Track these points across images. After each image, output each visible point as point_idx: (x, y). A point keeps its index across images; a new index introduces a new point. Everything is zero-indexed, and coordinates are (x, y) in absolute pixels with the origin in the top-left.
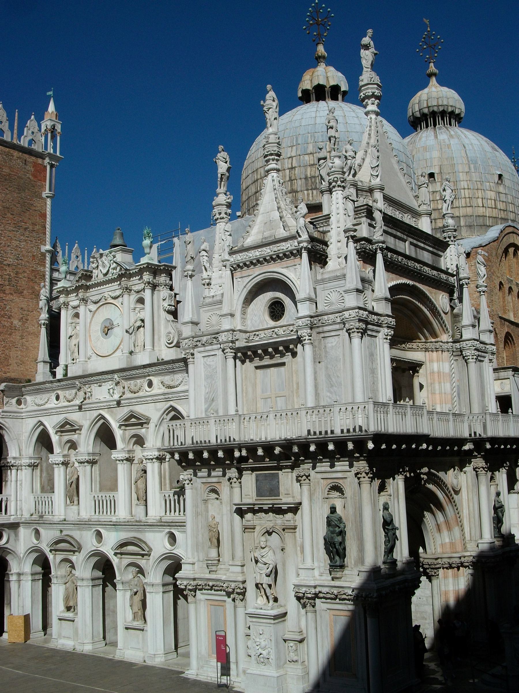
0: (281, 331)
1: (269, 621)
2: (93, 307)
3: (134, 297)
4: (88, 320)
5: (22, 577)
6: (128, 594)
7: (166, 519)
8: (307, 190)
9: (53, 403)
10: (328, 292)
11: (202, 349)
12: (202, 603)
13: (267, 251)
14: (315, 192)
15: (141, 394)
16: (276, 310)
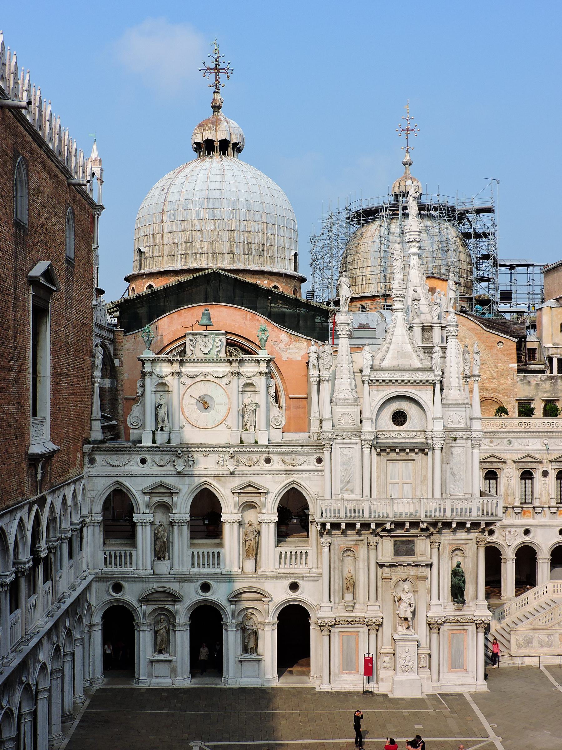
0: (405, 436)
1: (413, 643)
2: (189, 382)
3: (243, 381)
4: (182, 393)
5: (95, 629)
6: (239, 633)
7: (281, 571)
8: (244, 254)
9: (134, 465)
10: (451, 413)
11: (340, 442)
12: (336, 635)
13: (406, 376)
14: (250, 257)
15: (256, 468)
16: (399, 418)
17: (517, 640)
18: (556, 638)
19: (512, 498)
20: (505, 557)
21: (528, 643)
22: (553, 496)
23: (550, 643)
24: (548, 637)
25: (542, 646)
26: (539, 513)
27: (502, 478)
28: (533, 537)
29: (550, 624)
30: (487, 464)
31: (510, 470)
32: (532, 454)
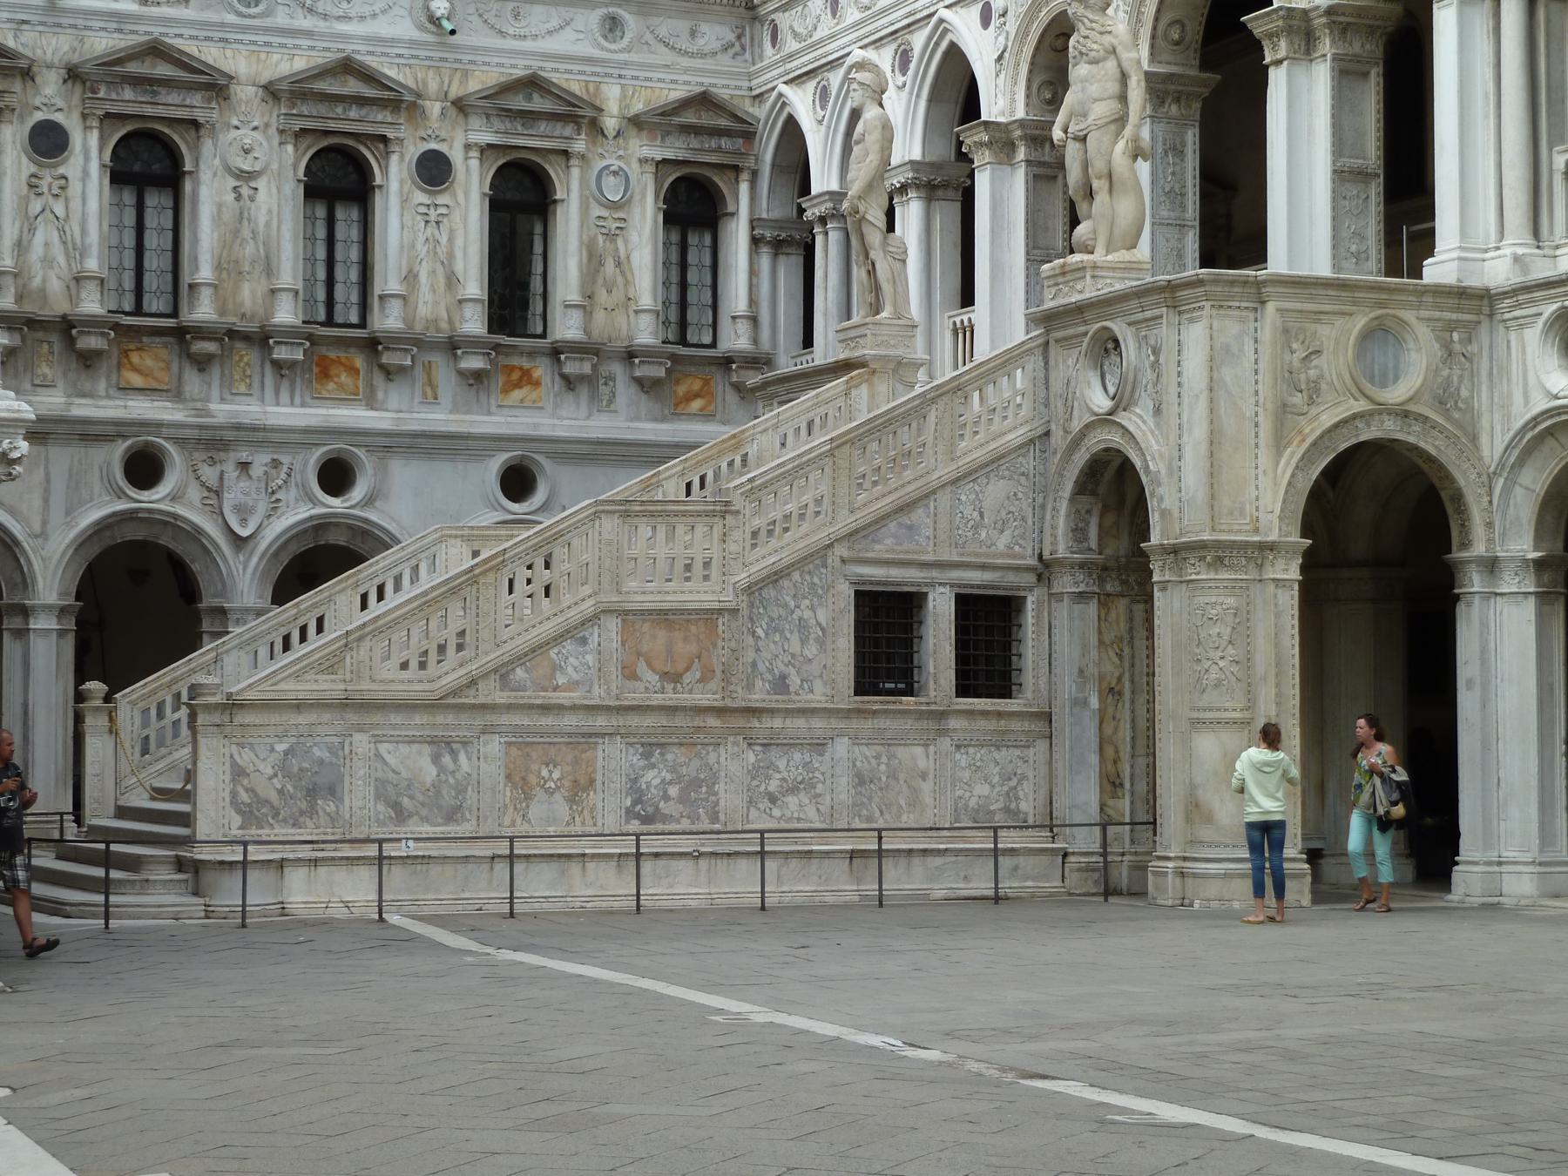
17: (238, 773)
18: (487, 760)
19: (262, 287)
20: (216, 602)
21: (312, 793)
22: (475, 285)
23: (448, 799)
24: (436, 759)
25: (401, 815)
26: (402, 370)
27: (205, 175)
28: (369, 501)
29: (449, 674)
30: (128, 94)
31: (247, 137)
32: (372, 62)
